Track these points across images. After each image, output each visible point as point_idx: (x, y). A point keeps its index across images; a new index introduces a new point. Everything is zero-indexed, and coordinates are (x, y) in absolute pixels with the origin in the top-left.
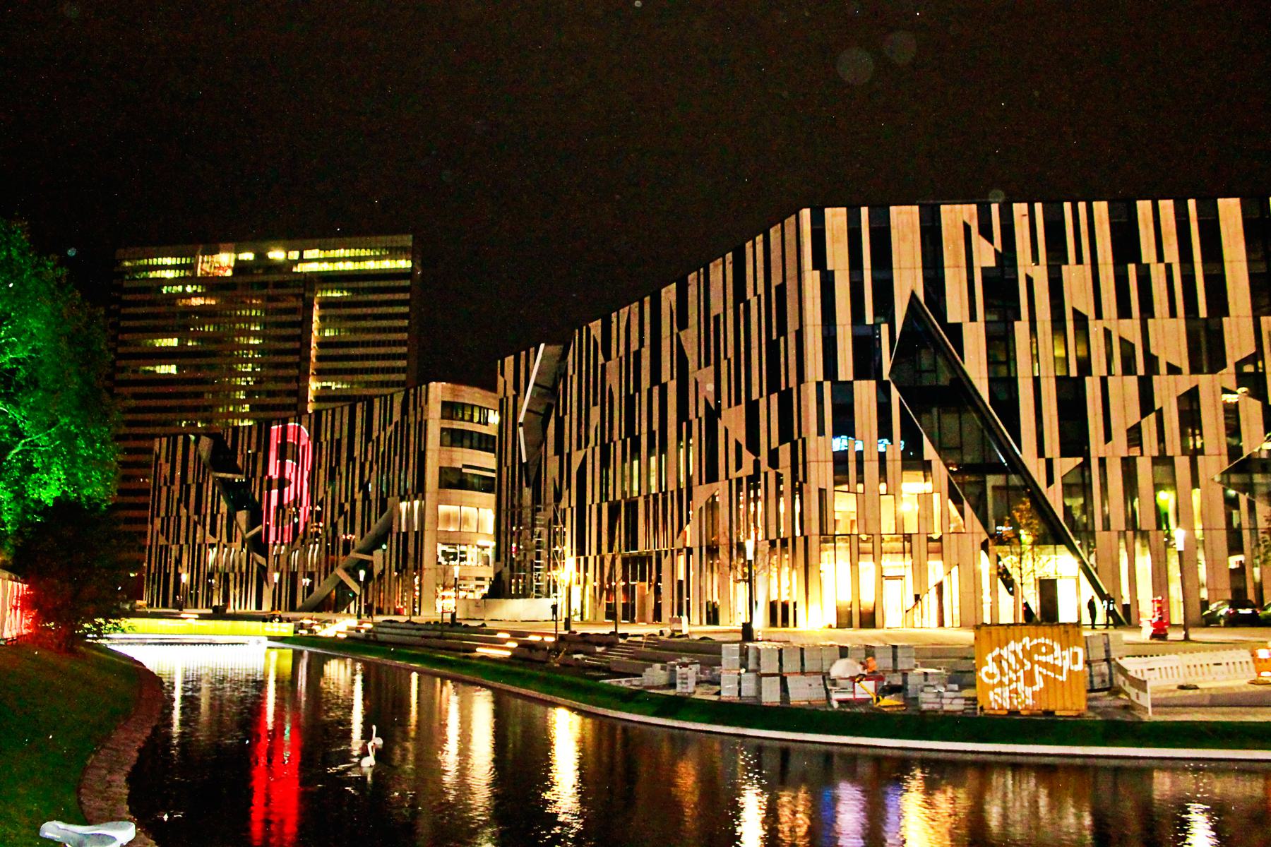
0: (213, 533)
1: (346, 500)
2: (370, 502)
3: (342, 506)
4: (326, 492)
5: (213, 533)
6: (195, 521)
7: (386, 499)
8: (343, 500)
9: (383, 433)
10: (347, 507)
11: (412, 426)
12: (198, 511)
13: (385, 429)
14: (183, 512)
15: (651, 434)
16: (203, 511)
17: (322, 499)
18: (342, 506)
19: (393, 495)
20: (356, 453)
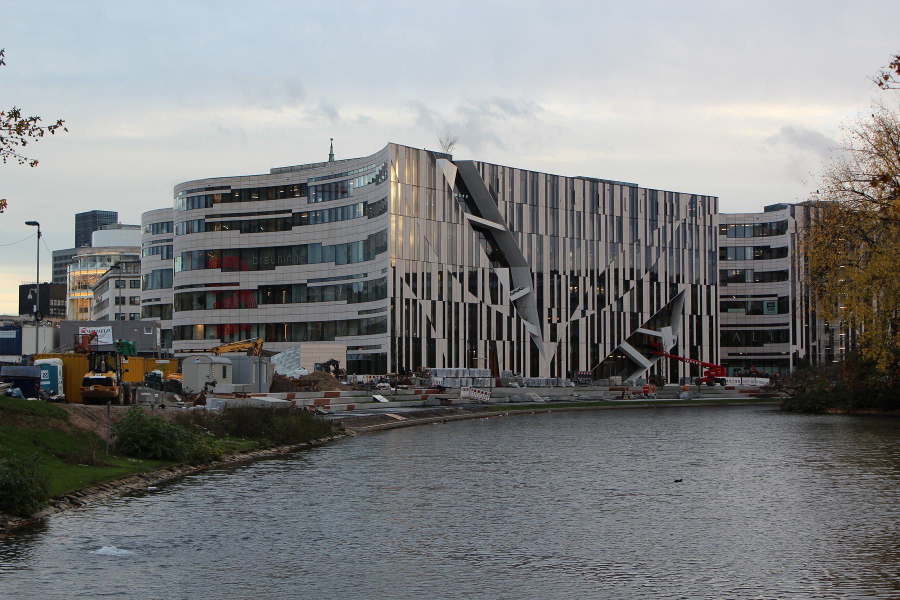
0: (473, 289)
1: (632, 278)
2: (659, 285)
3: (626, 284)
4: (607, 266)
5: (473, 289)
6: (449, 273)
8: (628, 278)
9: (669, 226)
10: (633, 284)
13: (671, 222)
14: (433, 258)
15: (698, 256)
17: (604, 273)
18: (626, 284)
19: (683, 282)
20: (641, 236)
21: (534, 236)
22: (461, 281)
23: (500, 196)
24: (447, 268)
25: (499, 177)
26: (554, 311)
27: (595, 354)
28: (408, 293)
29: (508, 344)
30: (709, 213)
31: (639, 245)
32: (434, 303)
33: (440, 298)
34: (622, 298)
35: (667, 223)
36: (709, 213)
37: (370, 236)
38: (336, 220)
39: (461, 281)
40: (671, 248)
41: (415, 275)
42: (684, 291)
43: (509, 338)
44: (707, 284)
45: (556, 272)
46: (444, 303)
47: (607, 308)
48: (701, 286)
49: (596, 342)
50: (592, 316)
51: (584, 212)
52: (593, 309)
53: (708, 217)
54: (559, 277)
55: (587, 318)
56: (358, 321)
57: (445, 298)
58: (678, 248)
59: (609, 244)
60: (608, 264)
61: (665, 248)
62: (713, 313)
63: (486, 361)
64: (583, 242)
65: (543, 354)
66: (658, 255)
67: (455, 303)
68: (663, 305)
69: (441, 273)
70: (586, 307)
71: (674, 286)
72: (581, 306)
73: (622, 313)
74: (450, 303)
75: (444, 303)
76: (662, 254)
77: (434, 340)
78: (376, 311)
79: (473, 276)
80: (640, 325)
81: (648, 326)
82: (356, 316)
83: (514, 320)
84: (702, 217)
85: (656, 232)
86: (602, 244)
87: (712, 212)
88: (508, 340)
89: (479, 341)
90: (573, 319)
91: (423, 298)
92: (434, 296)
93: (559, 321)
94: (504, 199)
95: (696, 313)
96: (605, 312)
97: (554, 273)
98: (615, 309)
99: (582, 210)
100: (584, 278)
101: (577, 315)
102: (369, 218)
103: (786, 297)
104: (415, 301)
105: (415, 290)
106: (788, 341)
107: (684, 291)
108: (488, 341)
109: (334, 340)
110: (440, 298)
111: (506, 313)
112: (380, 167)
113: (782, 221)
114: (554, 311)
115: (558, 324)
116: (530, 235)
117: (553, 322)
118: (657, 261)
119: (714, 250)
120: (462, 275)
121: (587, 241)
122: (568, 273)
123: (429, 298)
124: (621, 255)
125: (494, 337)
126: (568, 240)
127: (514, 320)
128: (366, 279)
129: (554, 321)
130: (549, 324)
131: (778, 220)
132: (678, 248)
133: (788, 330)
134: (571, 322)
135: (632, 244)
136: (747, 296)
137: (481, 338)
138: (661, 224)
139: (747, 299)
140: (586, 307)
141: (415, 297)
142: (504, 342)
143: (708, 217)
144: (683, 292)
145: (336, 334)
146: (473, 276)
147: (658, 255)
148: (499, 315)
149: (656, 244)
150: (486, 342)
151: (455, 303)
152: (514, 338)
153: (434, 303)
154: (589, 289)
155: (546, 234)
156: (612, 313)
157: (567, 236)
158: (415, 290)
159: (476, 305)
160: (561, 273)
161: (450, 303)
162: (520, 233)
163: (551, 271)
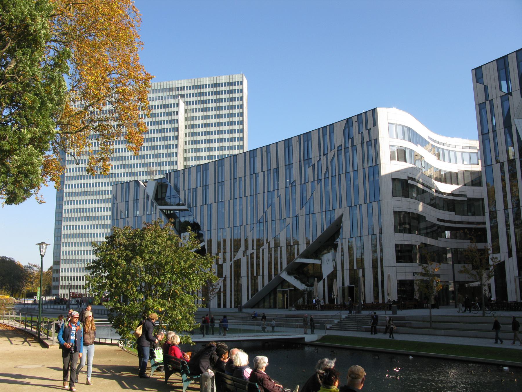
4: (265, 212)
11: (359, 147)
42: (342, 215)
47: (265, 246)
49: (255, 274)
50: (252, 254)
52: (253, 249)
55: (248, 256)
60: (266, 209)
66: (313, 189)
70: (247, 248)
72: (242, 248)
80: (296, 256)
81: (305, 255)
90: (236, 259)
96: (263, 250)
101: (239, 255)
107: (342, 215)
117: (220, 263)
118: (312, 194)
129: (221, 262)
130: (217, 265)
134: (235, 262)
140: (247, 248)
144: (341, 217)
147: (313, 189)
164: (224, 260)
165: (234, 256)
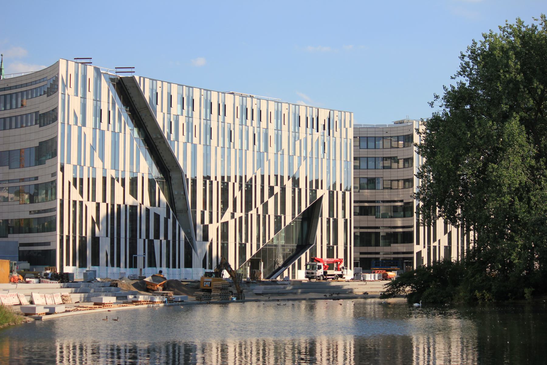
0: (134, 193)
2: (300, 190)
3: (271, 189)
5: (134, 193)
7: (316, 191)
8: (272, 184)
9: (309, 137)
10: (277, 190)
12: (115, 165)
14: (98, 163)
16: (121, 168)
17: (251, 179)
18: (271, 189)
19: (322, 188)
20: (285, 146)
21: (189, 145)
22: (123, 185)
23: (159, 108)
24: (111, 173)
25: (158, 91)
26: (207, 213)
27: (243, 249)
28: (75, 195)
29: (164, 242)
30: (345, 127)
31: (283, 154)
32: (98, 206)
33: (104, 200)
34: (267, 202)
35: (308, 135)
36: (345, 127)
37: (40, 143)
38: (11, 128)
39: (123, 185)
40: (311, 158)
41: (81, 180)
43: (166, 237)
44: (343, 190)
45: (209, 178)
46: (107, 204)
47: (253, 212)
48: (337, 192)
50: (241, 218)
51: (234, 124)
52: (242, 212)
53: (344, 130)
54: (211, 183)
55: (236, 220)
56: (28, 221)
57: (108, 200)
58: (317, 158)
59: (256, 153)
60: (255, 171)
61: (306, 158)
62: (347, 217)
63: (144, 258)
64: (233, 151)
65: (196, 252)
66: (300, 164)
67: (118, 205)
68: (303, 209)
69: (104, 179)
71: (314, 193)
73: (267, 216)
74: (113, 205)
75: (107, 204)
76: (303, 163)
77: (98, 238)
78: (45, 211)
79: (134, 181)
82: (28, 216)
83: (170, 221)
84: (338, 129)
85: (298, 143)
86: (250, 153)
87: (347, 125)
88: (165, 239)
89: (138, 240)
90: (224, 220)
91: (88, 200)
92: (99, 198)
93: (211, 222)
94: (162, 111)
95: (333, 216)
96: (251, 215)
97: (207, 178)
98: (261, 212)
99: (232, 123)
100: (234, 184)
101: (227, 216)
102: (40, 126)
103: (411, 202)
104: (81, 203)
105: (81, 193)
106: (412, 241)
108: (147, 240)
109: (7, 237)
110: (104, 200)
111: (163, 215)
112: (52, 80)
113: (408, 135)
114: (207, 213)
115: (210, 226)
116: (185, 144)
118: (299, 169)
119: (349, 160)
120: (123, 180)
121: (236, 150)
122: (219, 179)
123: (94, 200)
124: (266, 163)
125: (152, 237)
126: (219, 149)
127: (170, 221)
128: (36, 182)
131: (405, 134)
132: (317, 158)
133: (413, 232)
134: (221, 223)
135: (276, 154)
136: (378, 202)
137: (140, 238)
138: (302, 136)
139: (377, 204)
141: (81, 199)
142: (161, 241)
143: (344, 130)
144: (321, 198)
145: (9, 233)
146: (134, 181)
147: (300, 164)
148: (157, 217)
149: (298, 153)
150: (144, 240)
151: (118, 205)
152: (170, 237)
153: (98, 205)
154: (238, 194)
155: (200, 143)
156: (259, 216)
157: (218, 145)
158: (81, 193)
159: (136, 207)
160: (213, 178)
161: (113, 205)
162: (176, 142)
163: (204, 177)
164: (211, 222)
165: (222, 217)
